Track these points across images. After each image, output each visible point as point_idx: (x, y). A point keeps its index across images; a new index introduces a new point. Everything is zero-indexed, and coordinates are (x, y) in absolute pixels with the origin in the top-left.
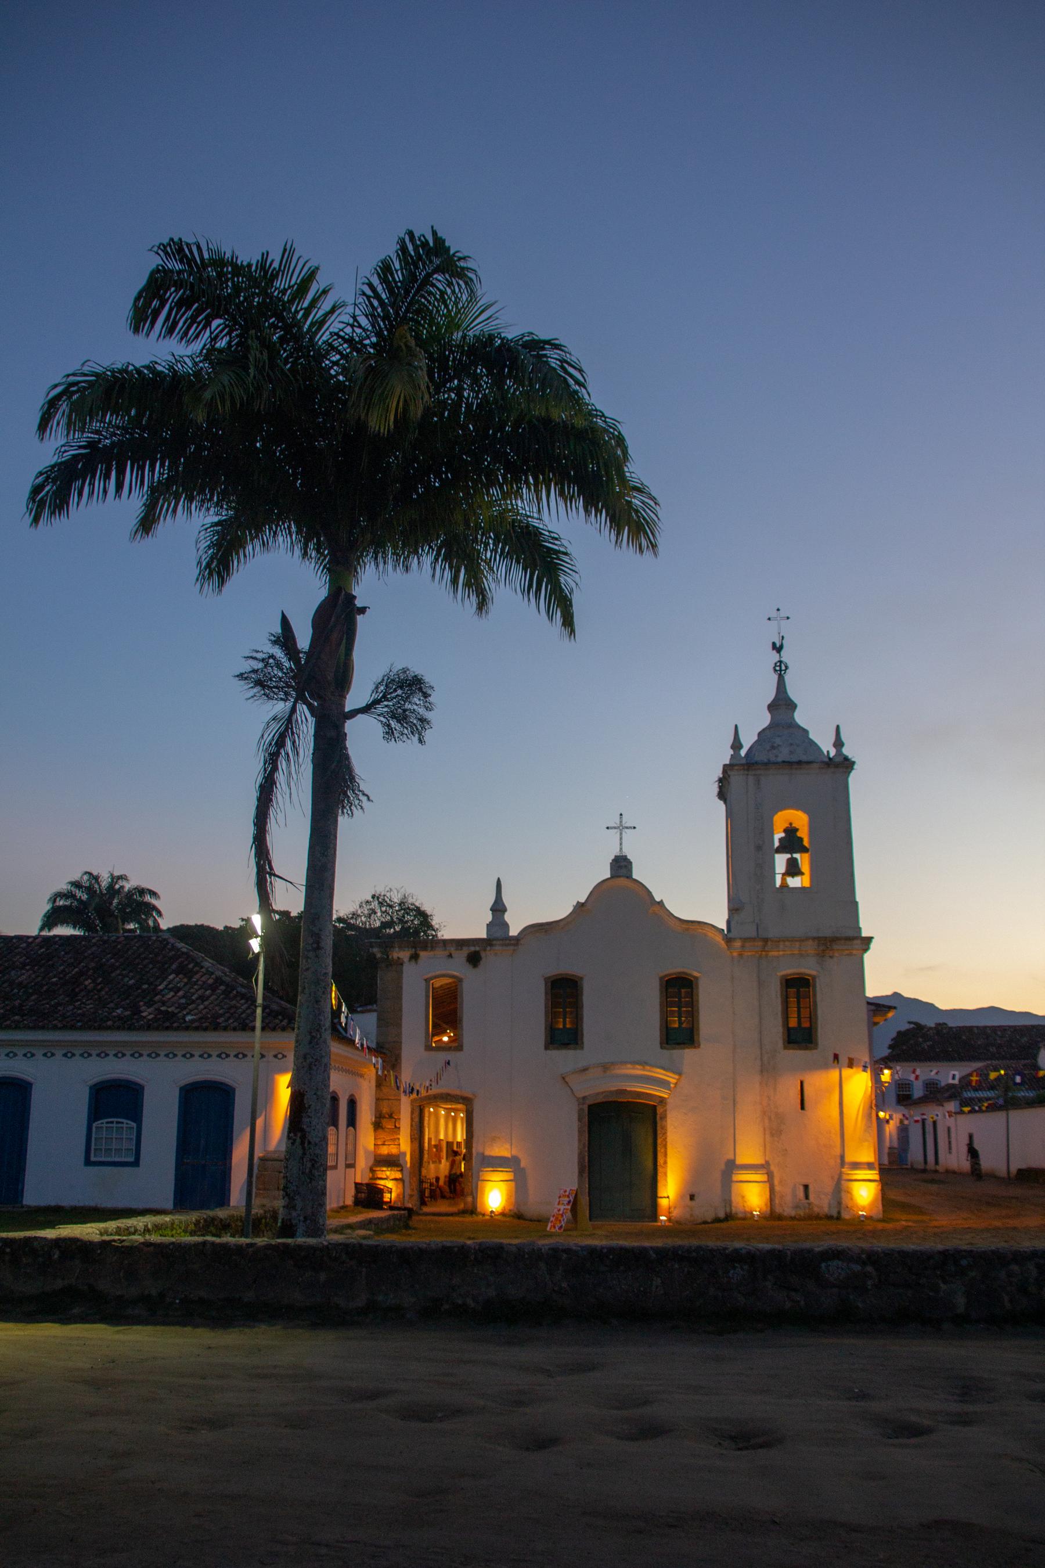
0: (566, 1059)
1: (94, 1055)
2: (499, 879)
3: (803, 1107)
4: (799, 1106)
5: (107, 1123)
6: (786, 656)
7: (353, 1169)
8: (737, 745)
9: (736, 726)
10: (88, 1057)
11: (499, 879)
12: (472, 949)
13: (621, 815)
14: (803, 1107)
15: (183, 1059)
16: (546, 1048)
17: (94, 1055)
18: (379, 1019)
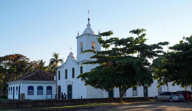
8: (78, 34)
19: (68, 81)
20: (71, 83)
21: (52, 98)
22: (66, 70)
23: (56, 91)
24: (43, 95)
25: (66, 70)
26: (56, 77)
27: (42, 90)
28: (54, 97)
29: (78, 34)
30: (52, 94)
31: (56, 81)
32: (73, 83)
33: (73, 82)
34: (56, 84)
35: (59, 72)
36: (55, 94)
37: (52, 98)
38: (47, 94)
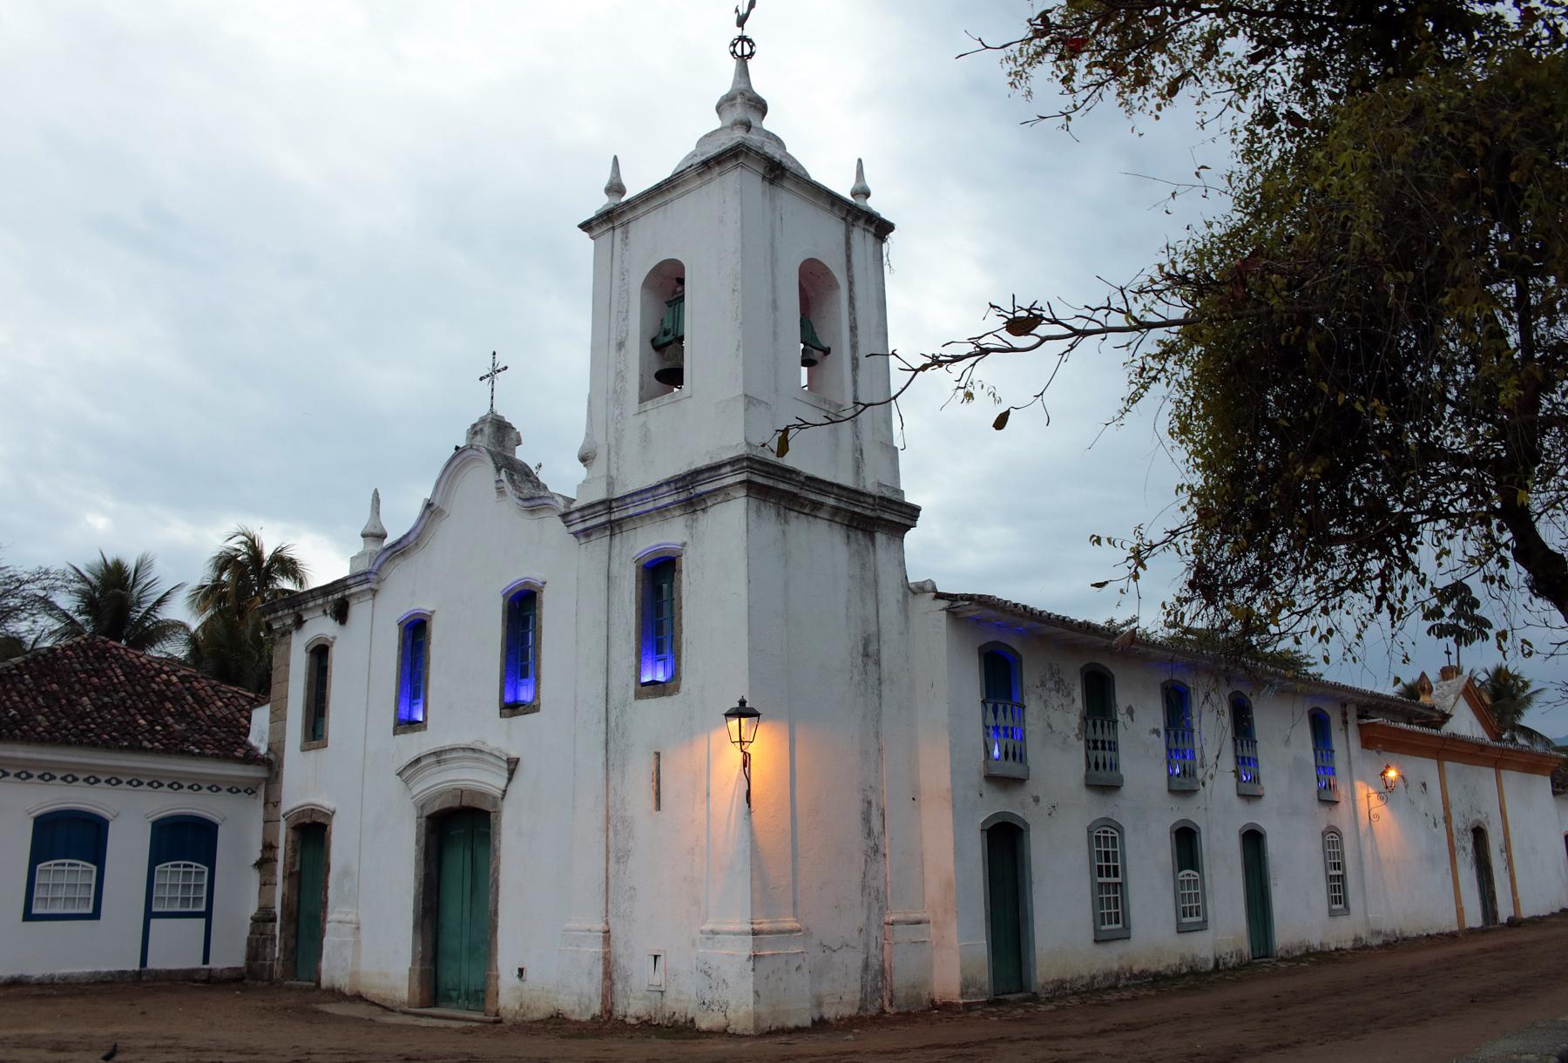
0: (415, 744)
1: (81, 780)
2: (376, 490)
3: (658, 808)
4: (652, 803)
5: (56, 865)
6: (749, 30)
7: (202, 921)
9: (615, 158)
10: (179, 788)
11: (376, 490)
12: (338, 596)
13: (494, 354)
14: (658, 808)
15: (85, 784)
16: (395, 733)
17: (81, 780)
18: (272, 712)
19: (439, 756)
20: (484, 779)
21: (206, 960)
22: (415, 632)
23: (267, 884)
24: (96, 915)
25: (415, 632)
26: (278, 717)
27: (97, 856)
28: (230, 954)
29: (616, 188)
30: (207, 915)
31: (271, 765)
32: (511, 773)
33: (513, 765)
34: (272, 802)
35: (320, 654)
36: (253, 909)
37: (206, 960)
38: (149, 915)
